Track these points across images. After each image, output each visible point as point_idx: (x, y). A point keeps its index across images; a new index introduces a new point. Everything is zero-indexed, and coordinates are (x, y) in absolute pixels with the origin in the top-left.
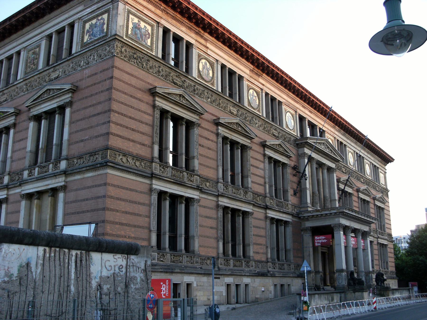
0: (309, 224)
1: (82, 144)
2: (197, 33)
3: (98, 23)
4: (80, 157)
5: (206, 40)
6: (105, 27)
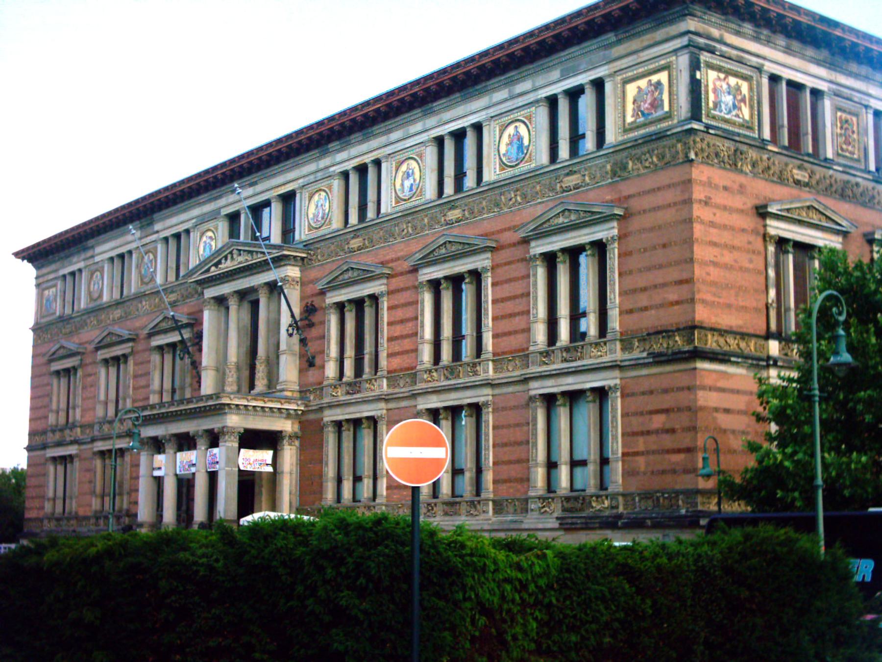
2: (86, 249)
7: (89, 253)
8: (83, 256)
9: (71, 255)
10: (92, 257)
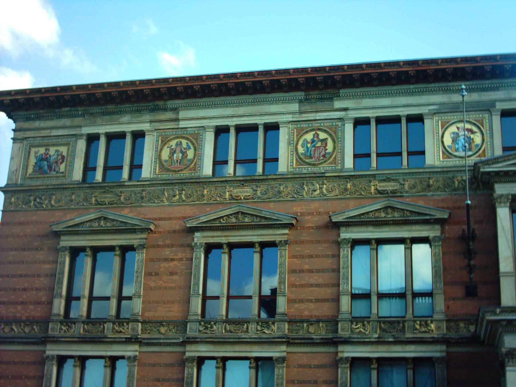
2: (155, 110)
5: (175, 110)
7: (170, 115)
8: (148, 117)
9: (120, 113)
10: (177, 120)
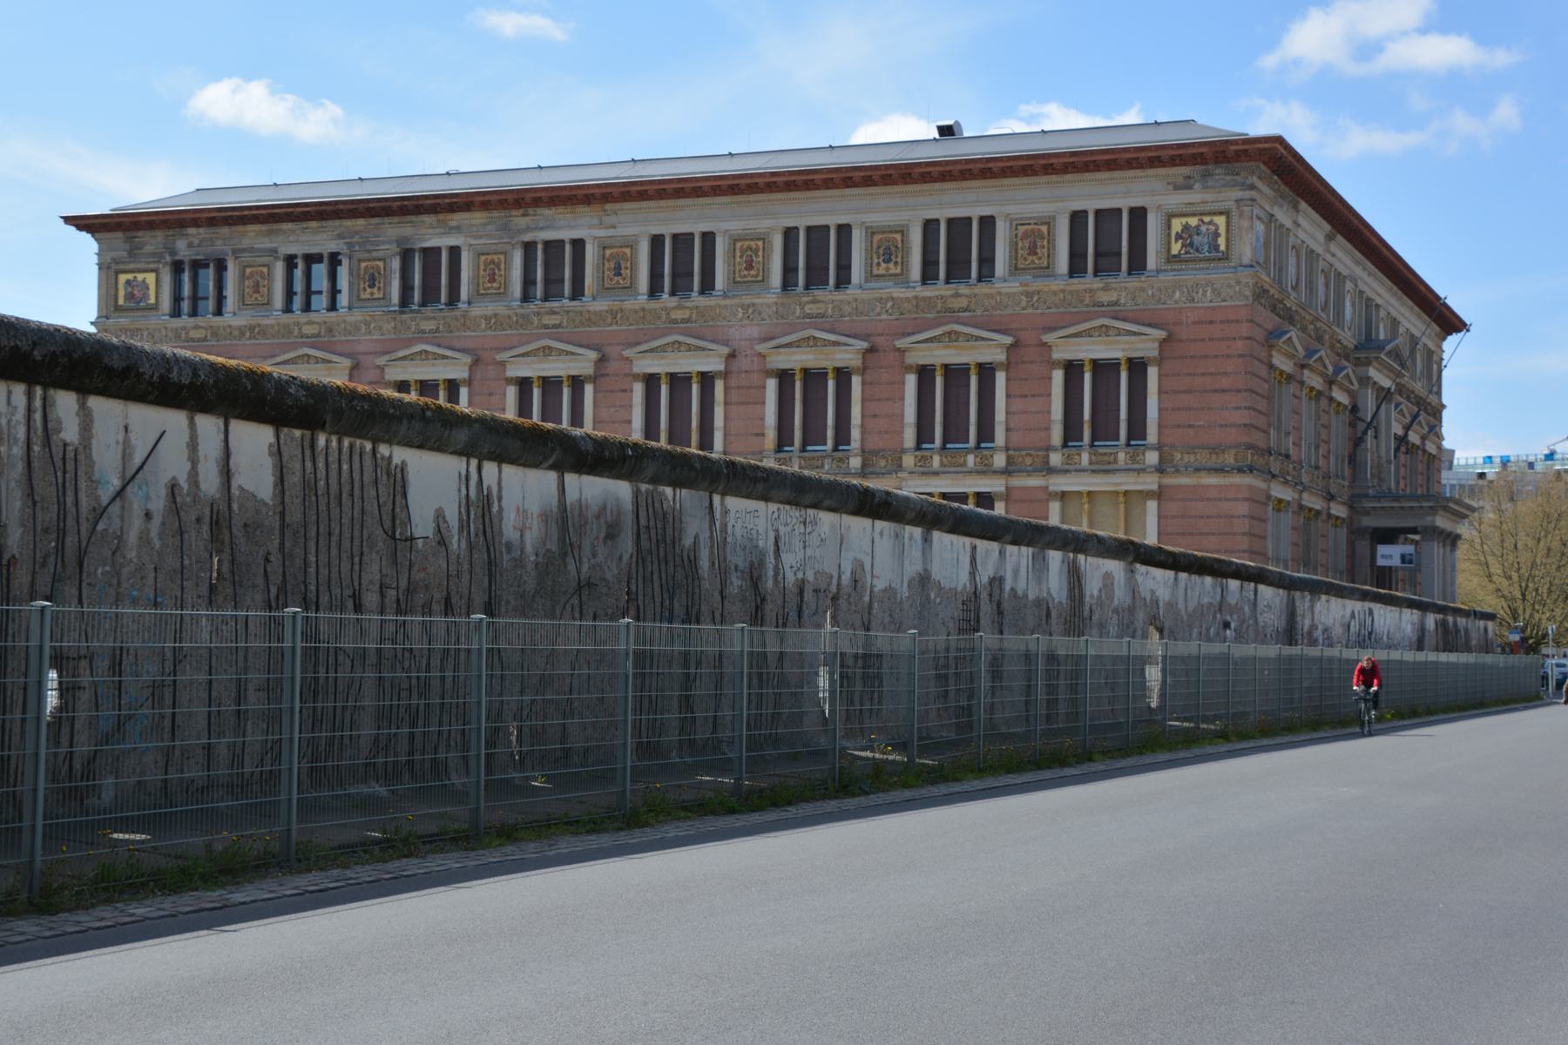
0: (1368, 522)
1: (1191, 432)
3: (1203, 228)
4: (1190, 449)
6: (1222, 241)
